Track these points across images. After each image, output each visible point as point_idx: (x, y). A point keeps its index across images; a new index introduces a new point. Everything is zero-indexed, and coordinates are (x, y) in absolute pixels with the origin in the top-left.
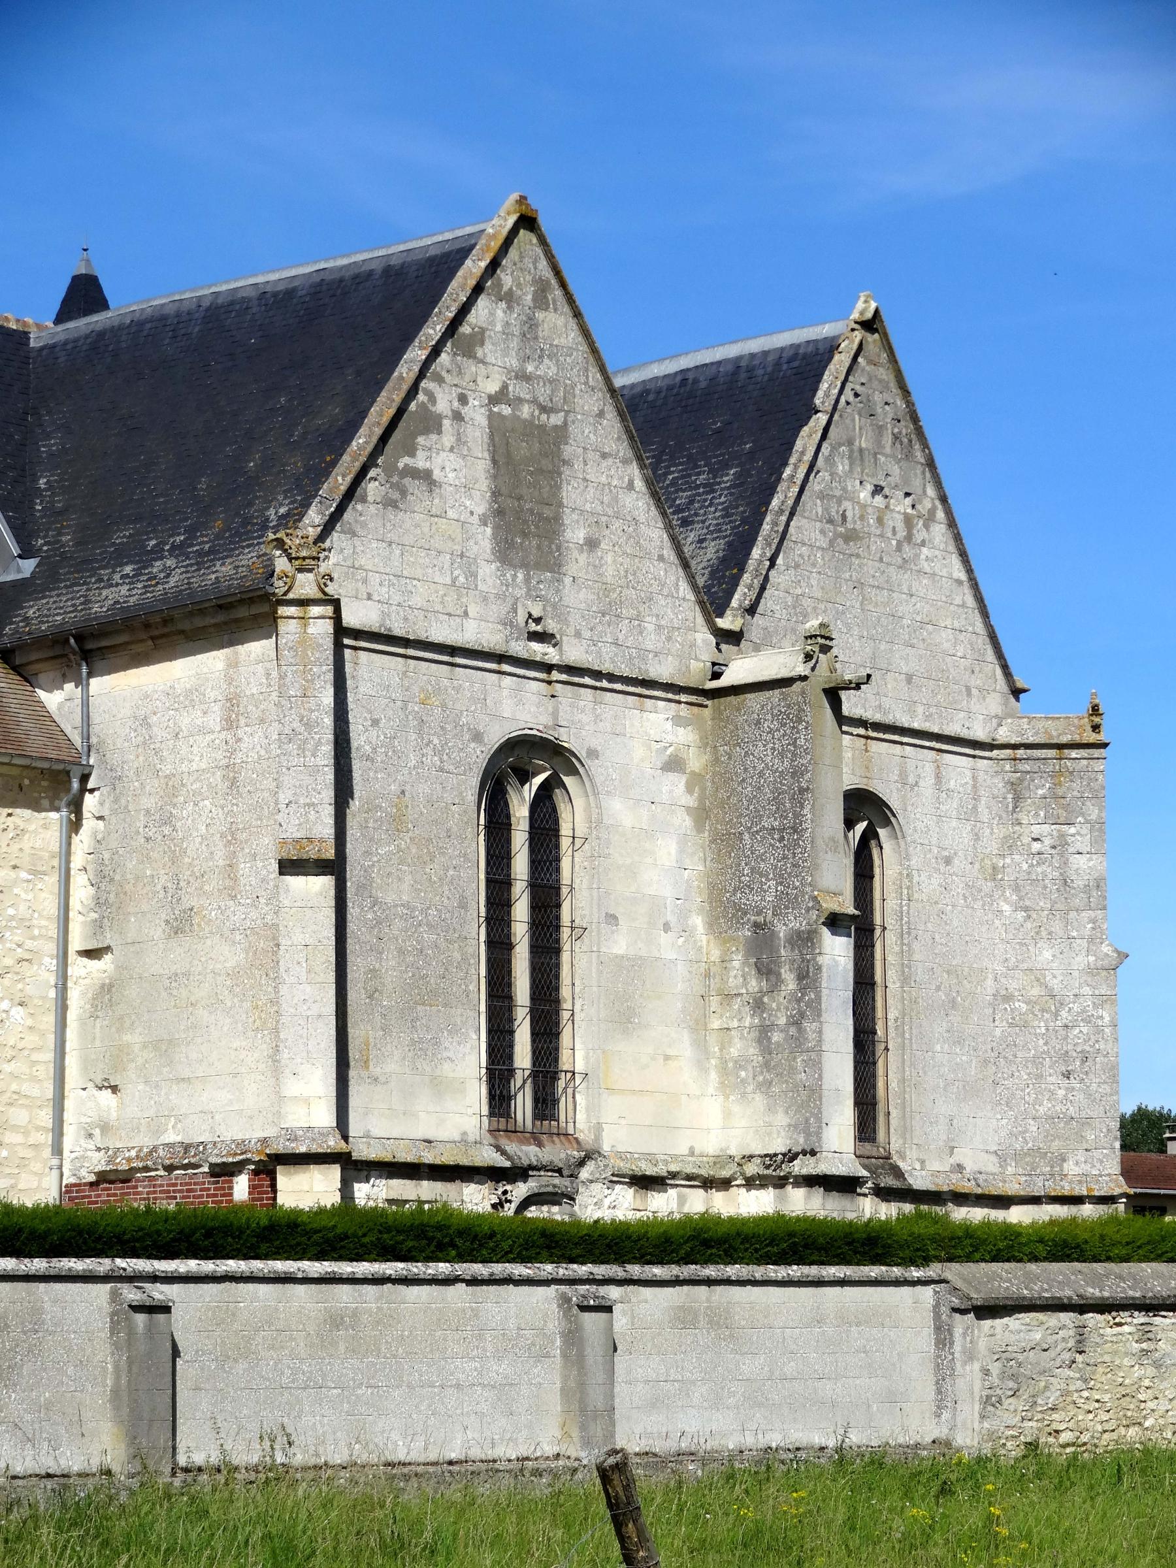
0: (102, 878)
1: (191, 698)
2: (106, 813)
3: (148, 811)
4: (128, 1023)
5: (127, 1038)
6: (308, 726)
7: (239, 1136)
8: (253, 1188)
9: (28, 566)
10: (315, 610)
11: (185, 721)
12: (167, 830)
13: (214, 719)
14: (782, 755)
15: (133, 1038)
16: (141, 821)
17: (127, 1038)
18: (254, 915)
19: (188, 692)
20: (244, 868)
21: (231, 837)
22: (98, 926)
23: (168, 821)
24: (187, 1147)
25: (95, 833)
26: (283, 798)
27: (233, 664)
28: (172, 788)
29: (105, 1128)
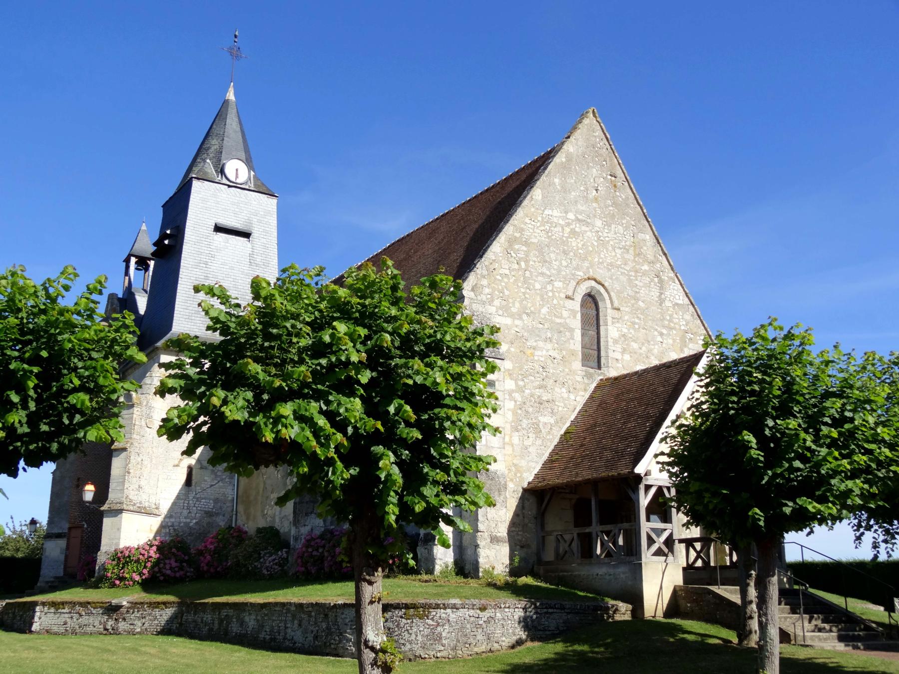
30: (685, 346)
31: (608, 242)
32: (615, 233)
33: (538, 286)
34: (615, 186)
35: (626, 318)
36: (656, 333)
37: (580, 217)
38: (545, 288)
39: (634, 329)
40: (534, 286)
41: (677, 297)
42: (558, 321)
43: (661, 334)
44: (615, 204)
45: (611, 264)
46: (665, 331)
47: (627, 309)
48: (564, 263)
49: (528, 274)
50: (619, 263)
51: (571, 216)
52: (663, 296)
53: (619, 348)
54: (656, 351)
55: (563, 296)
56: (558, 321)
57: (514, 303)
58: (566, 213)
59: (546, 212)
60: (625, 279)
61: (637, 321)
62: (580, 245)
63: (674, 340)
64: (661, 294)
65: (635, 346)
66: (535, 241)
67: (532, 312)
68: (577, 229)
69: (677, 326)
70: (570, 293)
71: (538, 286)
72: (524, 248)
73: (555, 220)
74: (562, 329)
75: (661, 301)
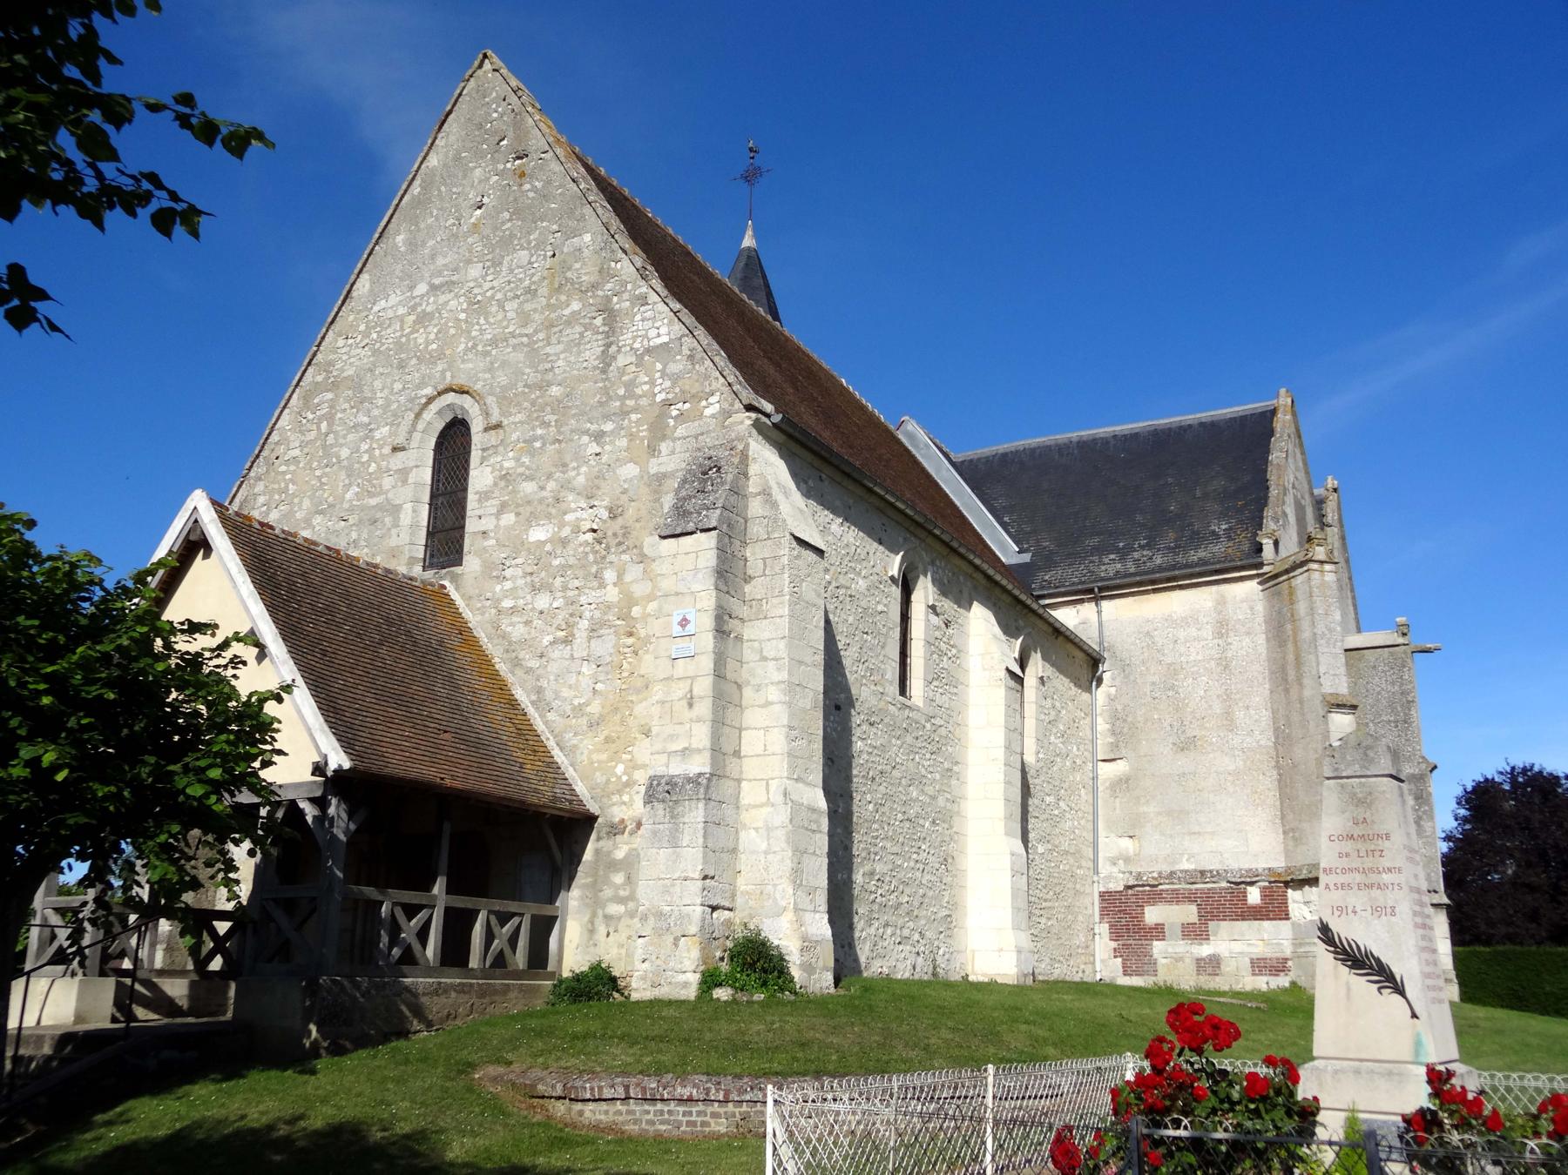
0: (1115, 718)
1: (1185, 622)
2: (1117, 683)
3: (1153, 683)
4: (1143, 800)
5: (1145, 809)
6: (1330, 630)
7: (1247, 866)
8: (1264, 897)
9: (1026, 558)
10: (1327, 567)
11: (1182, 634)
12: (1170, 693)
13: (1207, 632)
14: (1393, 683)
15: (1150, 809)
16: (1148, 689)
17: (1145, 809)
18: (1248, 740)
19: (1184, 619)
20: (1239, 714)
21: (1227, 697)
22: (1115, 746)
23: (1172, 688)
24: (1202, 873)
25: (1109, 696)
26: (1322, 670)
27: (1221, 601)
28: (1174, 670)
29: (1127, 860)
30: (664, 438)
31: (493, 297)
32: (511, 271)
33: (345, 453)
34: (523, 175)
35: (514, 437)
36: (586, 439)
37: (437, 281)
38: (358, 451)
39: (532, 453)
40: (338, 457)
41: (652, 333)
42: (373, 502)
43: (598, 437)
44: (517, 213)
45: (494, 342)
46: (608, 427)
47: (519, 417)
48: (398, 386)
49: (331, 439)
50: (511, 329)
51: (422, 288)
52: (614, 348)
53: (492, 506)
54: (581, 479)
55: (387, 450)
56: (373, 502)
57: (301, 503)
58: (412, 288)
59: (376, 308)
60: (521, 356)
61: (539, 432)
62: (432, 336)
63: (632, 437)
64: (608, 345)
65: (529, 487)
66: (351, 372)
67: (330, 506)
68: (429, 309)
69: (644, 402)
70: (400, 440)
71: (345, 453)
72: (330, 396)
73: (390, 314)
74: (379, 515)
75: (607, 359)
